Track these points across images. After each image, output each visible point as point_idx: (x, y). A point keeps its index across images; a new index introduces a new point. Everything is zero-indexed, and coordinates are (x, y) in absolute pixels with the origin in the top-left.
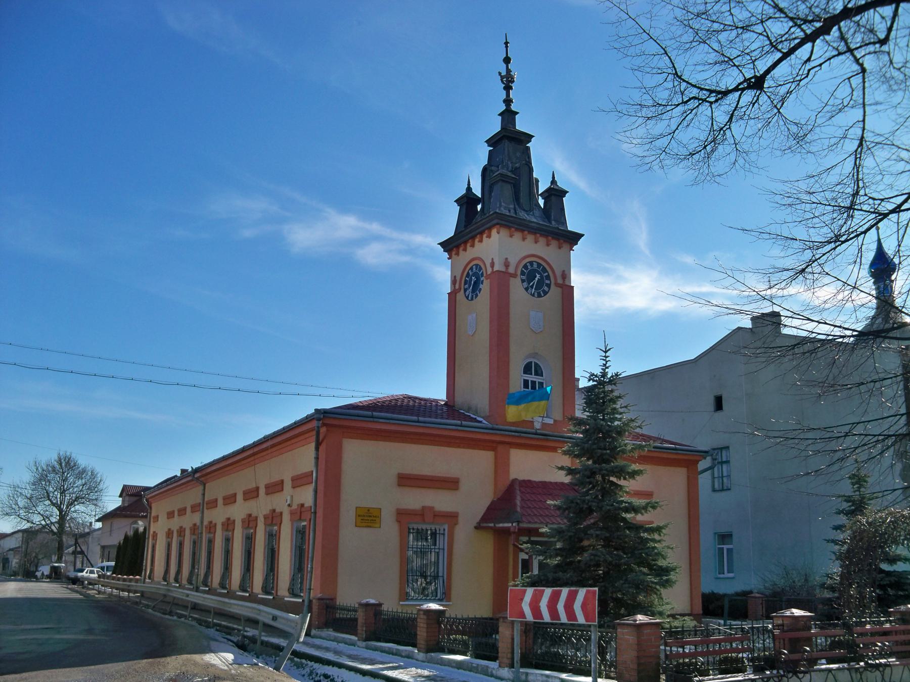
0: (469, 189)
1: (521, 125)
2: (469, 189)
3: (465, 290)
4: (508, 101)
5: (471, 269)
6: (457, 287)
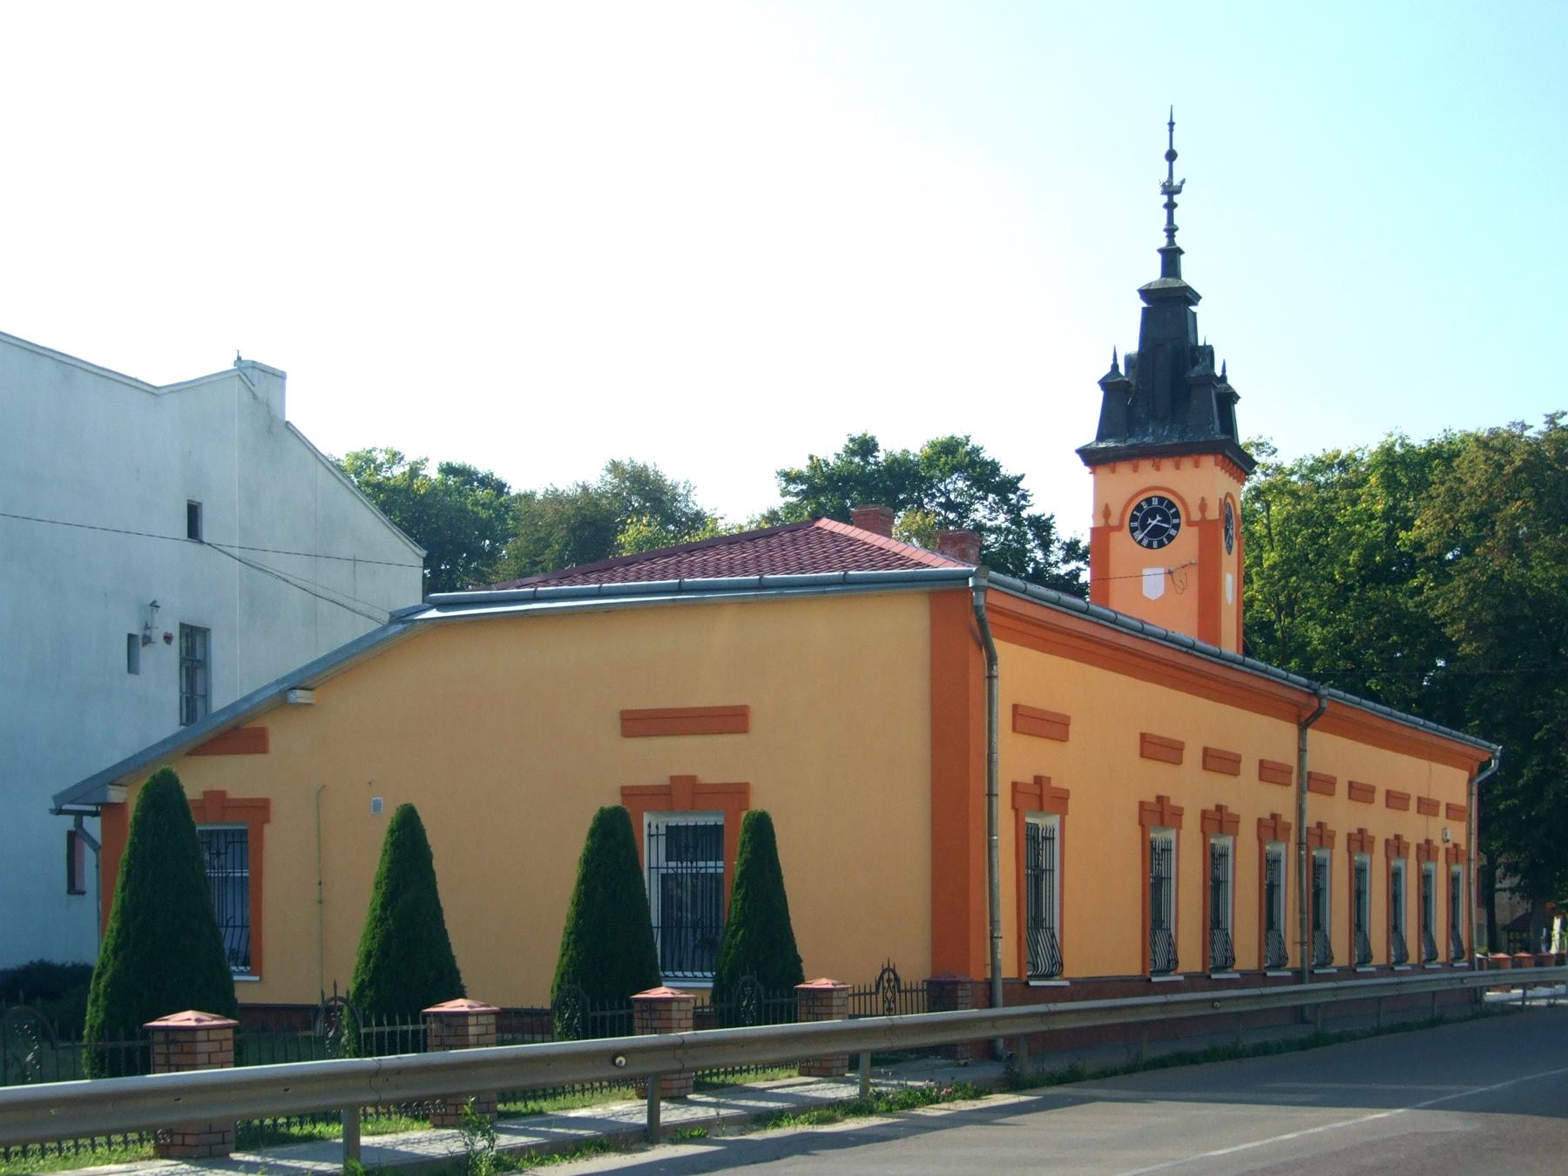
0: (1115, 367)
1: (1190, 274)
2: (1115, 367)
3: (1133, 530)
4: (1171, 230)
5: (1149, 501)
6: (1114, 521)
